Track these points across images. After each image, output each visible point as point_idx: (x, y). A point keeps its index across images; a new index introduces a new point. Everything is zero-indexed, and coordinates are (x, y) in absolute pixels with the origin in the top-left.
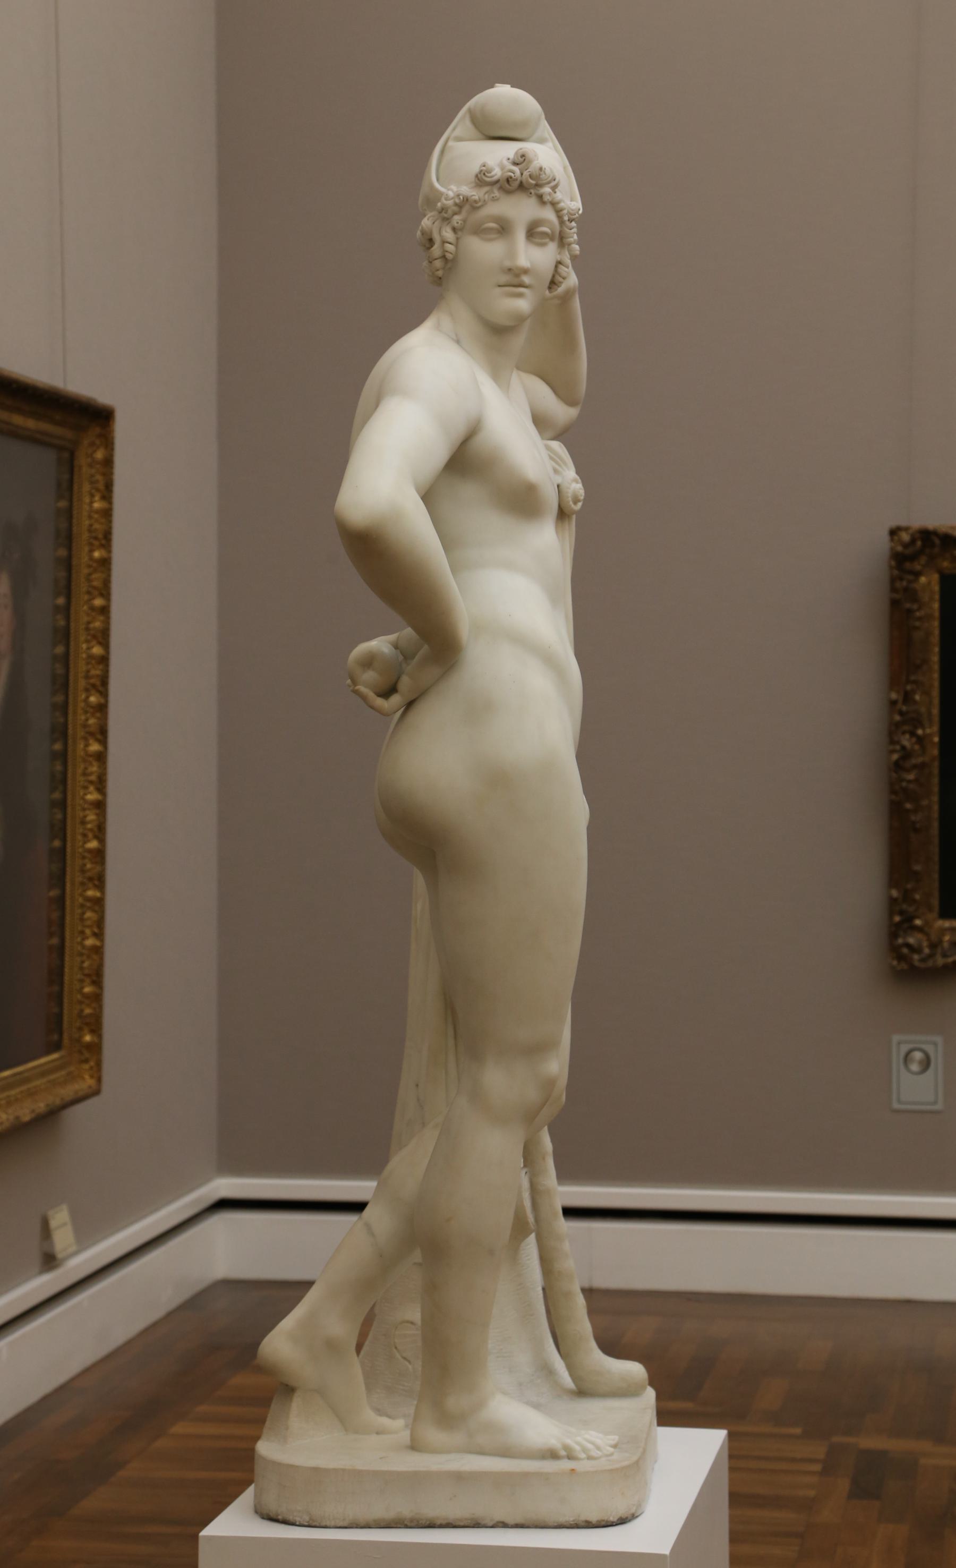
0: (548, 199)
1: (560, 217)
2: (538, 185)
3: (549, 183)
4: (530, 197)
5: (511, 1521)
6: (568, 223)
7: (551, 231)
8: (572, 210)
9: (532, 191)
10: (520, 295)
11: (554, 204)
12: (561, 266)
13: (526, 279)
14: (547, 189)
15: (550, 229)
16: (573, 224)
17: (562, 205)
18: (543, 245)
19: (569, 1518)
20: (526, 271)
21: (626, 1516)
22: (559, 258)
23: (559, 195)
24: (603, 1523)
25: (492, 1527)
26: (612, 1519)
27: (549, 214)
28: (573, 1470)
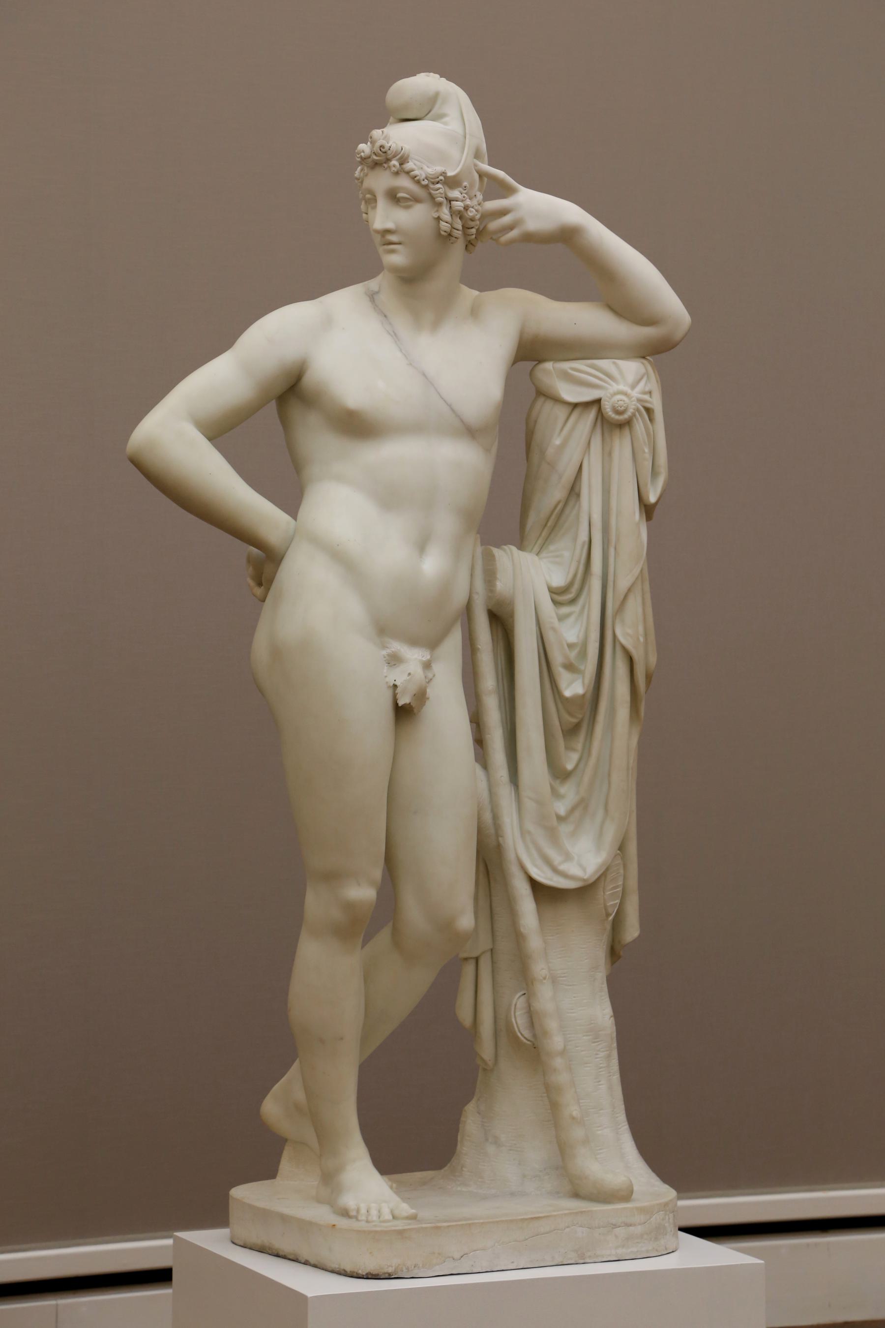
0: (394, 171)
1: (418, 182)
2: (388, 160)
3: (394, 156)
4: (386, 169)
5: (312, 1261)
6: (432, 186)
7: (411, 196)
8: (431, 175)
9: (386, 165)
10: (393, 251)
11: (408, 173)
12: (441, 222)
13: (393, 238)
14: (394, 162)
15: (406, 194)
16: (439, 186)
17: (416, 172)
18: (407, 207)
19: (335, 1266)
20: (388, 231)
21: (376, 1273)
22: (436, 215)
23: (409, 166)
24: (355, 1275)
25: (304, 1264)
26: (360, 1272)
27: (405, 182)
28: (334, 1225)
